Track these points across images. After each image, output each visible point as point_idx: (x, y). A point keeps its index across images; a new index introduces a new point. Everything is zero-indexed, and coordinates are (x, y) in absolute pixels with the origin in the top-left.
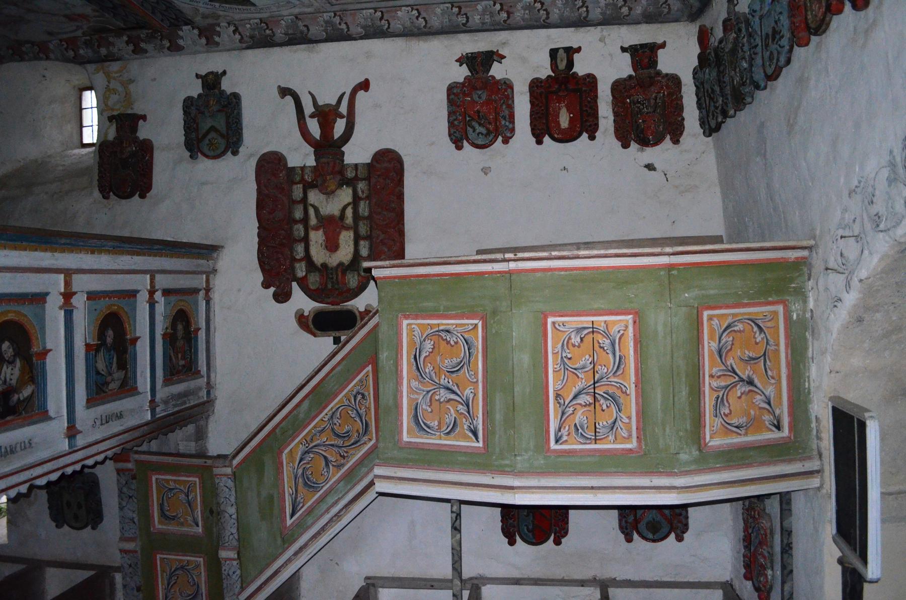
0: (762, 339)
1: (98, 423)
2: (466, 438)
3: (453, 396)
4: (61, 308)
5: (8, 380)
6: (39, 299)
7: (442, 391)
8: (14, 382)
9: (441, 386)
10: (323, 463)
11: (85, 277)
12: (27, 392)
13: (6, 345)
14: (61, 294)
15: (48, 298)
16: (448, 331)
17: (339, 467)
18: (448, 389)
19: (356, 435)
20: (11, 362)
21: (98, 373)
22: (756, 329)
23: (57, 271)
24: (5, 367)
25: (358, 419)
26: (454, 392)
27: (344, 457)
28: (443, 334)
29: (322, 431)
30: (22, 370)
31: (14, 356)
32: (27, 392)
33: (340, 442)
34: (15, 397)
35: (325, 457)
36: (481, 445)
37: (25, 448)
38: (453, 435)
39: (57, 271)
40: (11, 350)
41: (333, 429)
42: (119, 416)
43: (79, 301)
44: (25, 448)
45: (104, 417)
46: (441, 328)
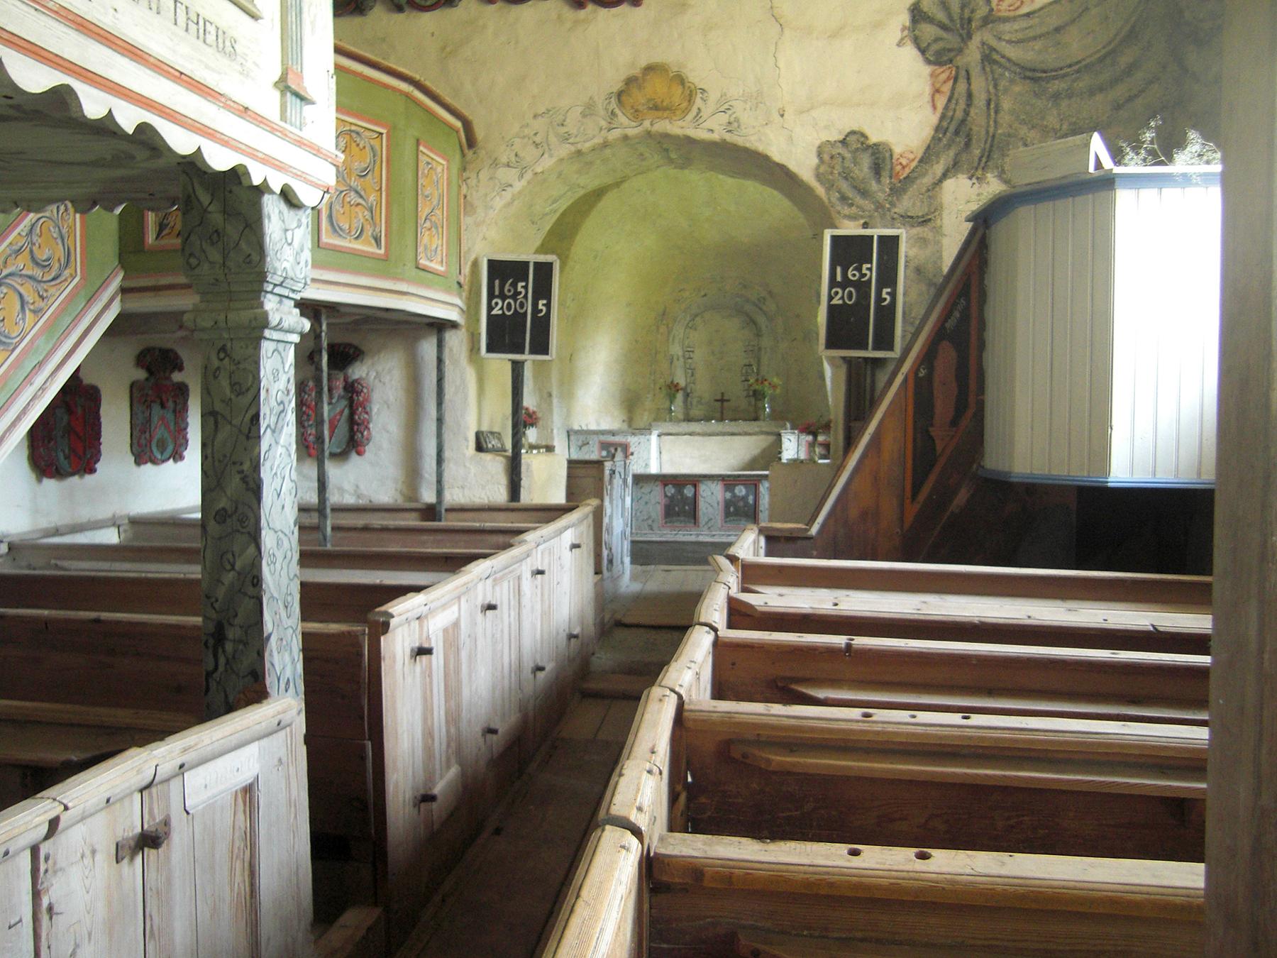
2: (370, 244)
3: (360, 201)
7: (352, 193)
9: (351, 188)
10: (18, 307)
16: (358, 133)
17: (37, 312)
18: (357, 192)
19: (57, 265)
25: (59, 241)
26: (361, 197)
27: (42, 298)
28: (354, 135)
29: (18, 252)
33: (38, 273)
35: (21, 296)
36: (382, 251)
38: (360, 240)
41: (31, 251)
46: (353, 128)
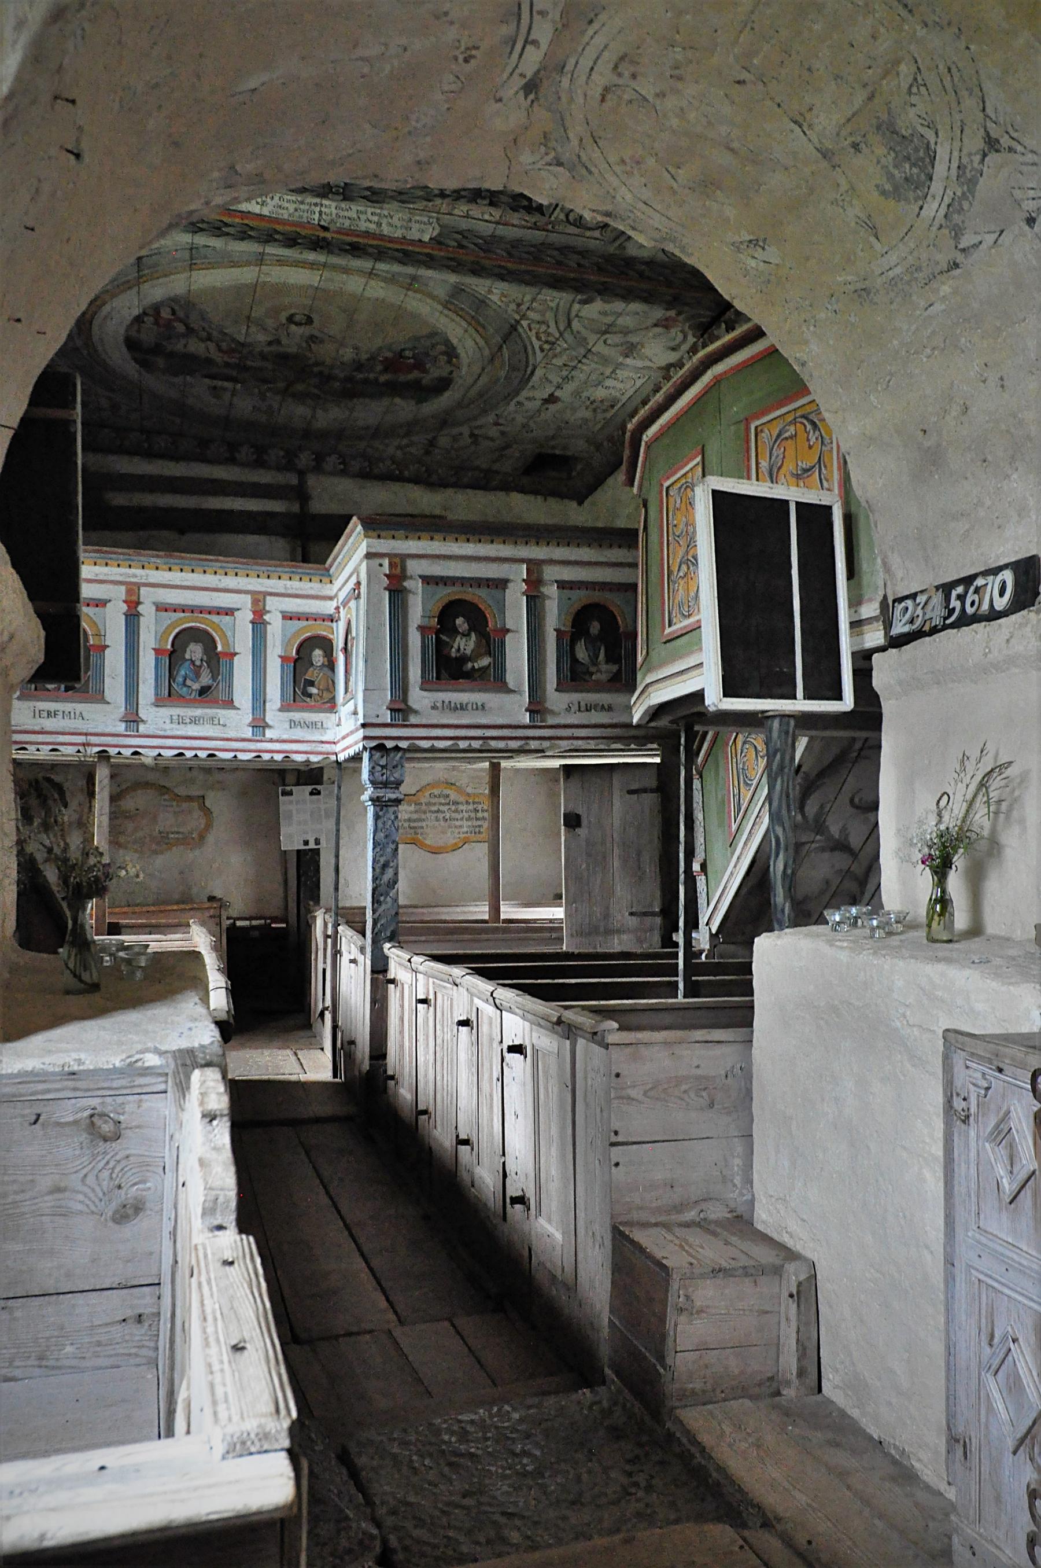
0: (817, 439)
1: (575, 708)
4: (523, 593)
5: (462, 648)
6: (501, 584)
8: (468, 652)
11: (557, 568)
12: (485, 661)
13: (459, 621)
14: (524, 580)
15: (510, 585)
20: (467, 635)
21: (575, 660)
22: (809, 427)
23: (522, 561)
24: (458, 639)
30: (478, 644)
31: (470, 630)
32: (485, 661)
34: (470, 665)
37: (477, 709)
39: (522, 561)
40: (466, 625)
42: (610, 709)
43: (551, 591)
44: (477, 709)
45: (583, 704)
